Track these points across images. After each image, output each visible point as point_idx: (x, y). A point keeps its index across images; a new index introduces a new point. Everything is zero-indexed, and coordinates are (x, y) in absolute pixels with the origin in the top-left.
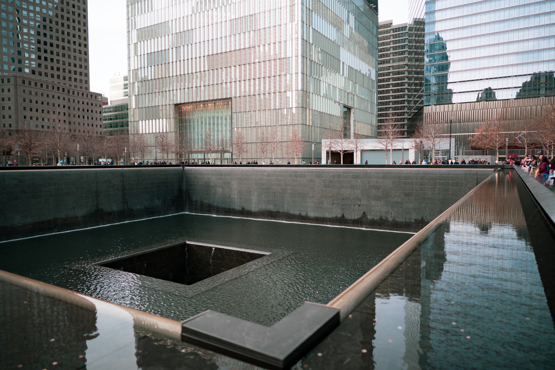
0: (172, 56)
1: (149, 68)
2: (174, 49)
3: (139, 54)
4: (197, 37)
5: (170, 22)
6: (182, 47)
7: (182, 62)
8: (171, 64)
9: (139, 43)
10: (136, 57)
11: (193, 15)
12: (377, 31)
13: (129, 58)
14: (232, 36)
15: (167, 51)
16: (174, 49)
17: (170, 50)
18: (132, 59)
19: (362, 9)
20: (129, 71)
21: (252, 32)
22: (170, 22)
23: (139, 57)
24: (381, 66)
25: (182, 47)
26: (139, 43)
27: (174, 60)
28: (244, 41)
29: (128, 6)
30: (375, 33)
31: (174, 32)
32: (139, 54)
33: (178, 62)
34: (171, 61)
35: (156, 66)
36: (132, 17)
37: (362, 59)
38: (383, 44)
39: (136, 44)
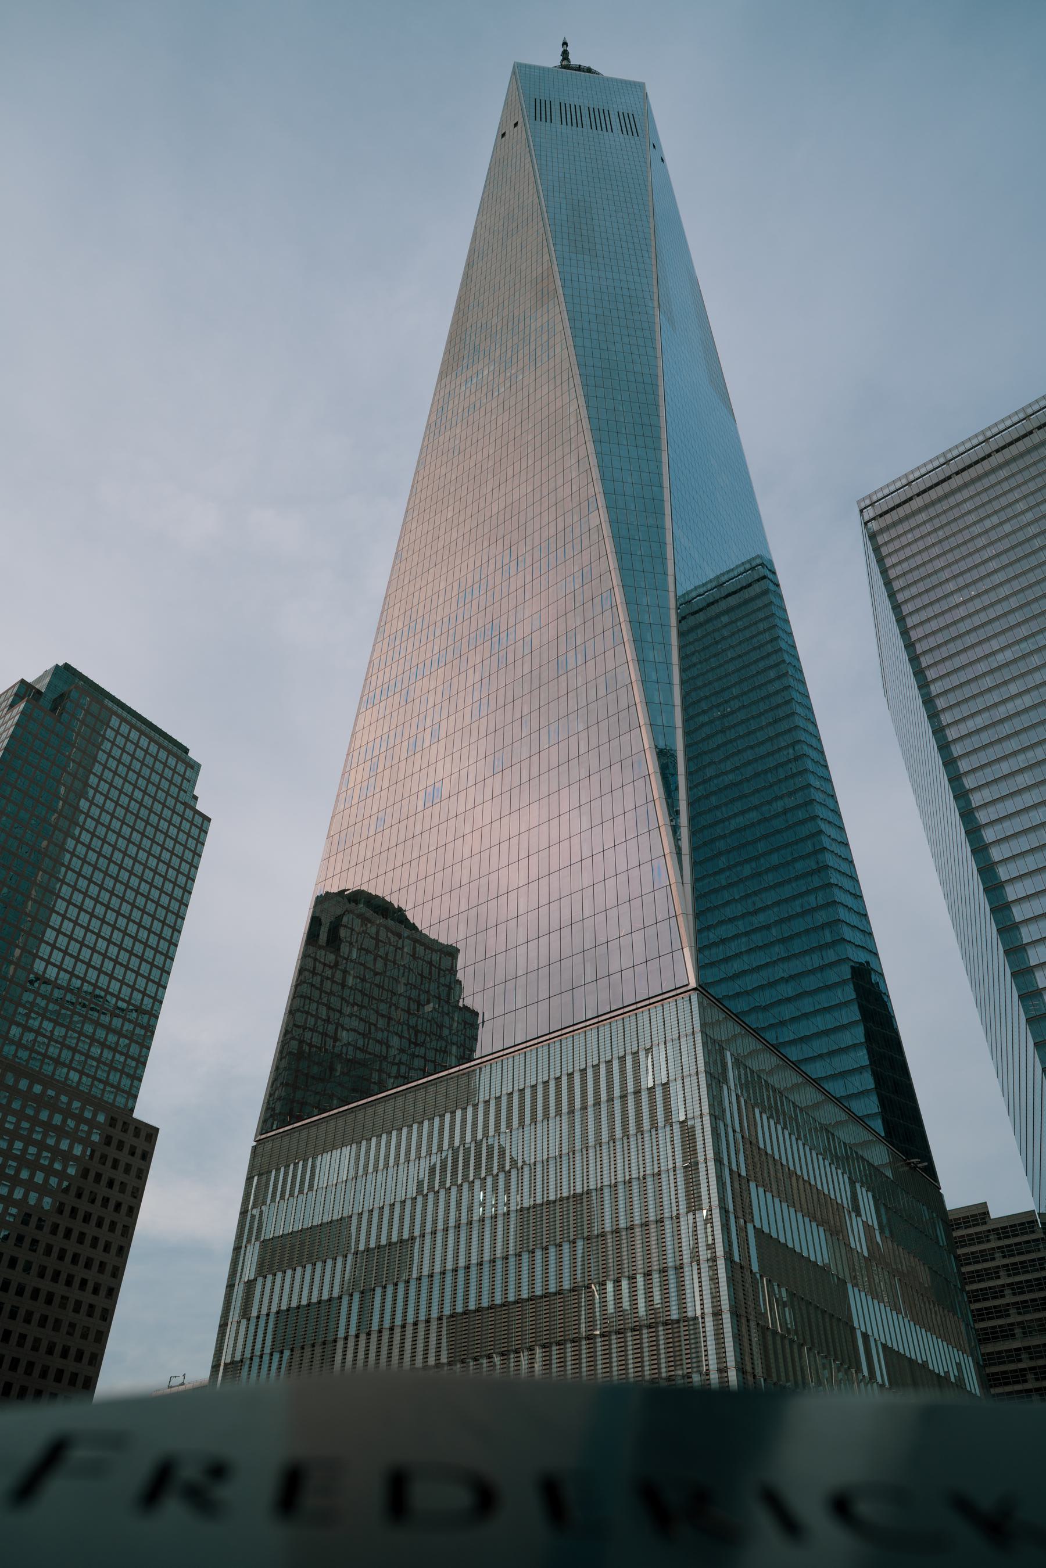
0: (347, 1320)
1: (276, 1356)
2: (356, 1297)
3: (254, 1314)
4: (425, 1260)
5: (355, 1219)
6: (379, 1291)
7: (374, 1337)
8: (340, 1344)
9: (260, 1280)
10: (244, 1322)
11: (420, 1199)
12: (948, 1236)
13: (223, 1326)
14: (525, 1256)
15: (335, 1303)
16: (356, 1297)
17: (345, 1299)
18: (231, 1330)
19: (889, 1174)
20: (215, 1367)
21: (580, 1244)
22: (355, 1219)
23: (253, 1321)
24: (989, 1348)
25: (379, 1291)
26: (260, 1280)
27: (353, 1331)
28: (556, 1270)
29: (249, 1179)
30: (943, 1241)
31: (362, 1248)
32: (254, 1314)
33: (363, 1337)
34: (341, 1334)
35: (297, 1353)
36: (254, 1207)
37: (916, 1320)
38: (979, 1276)
39: (250, 1284)
